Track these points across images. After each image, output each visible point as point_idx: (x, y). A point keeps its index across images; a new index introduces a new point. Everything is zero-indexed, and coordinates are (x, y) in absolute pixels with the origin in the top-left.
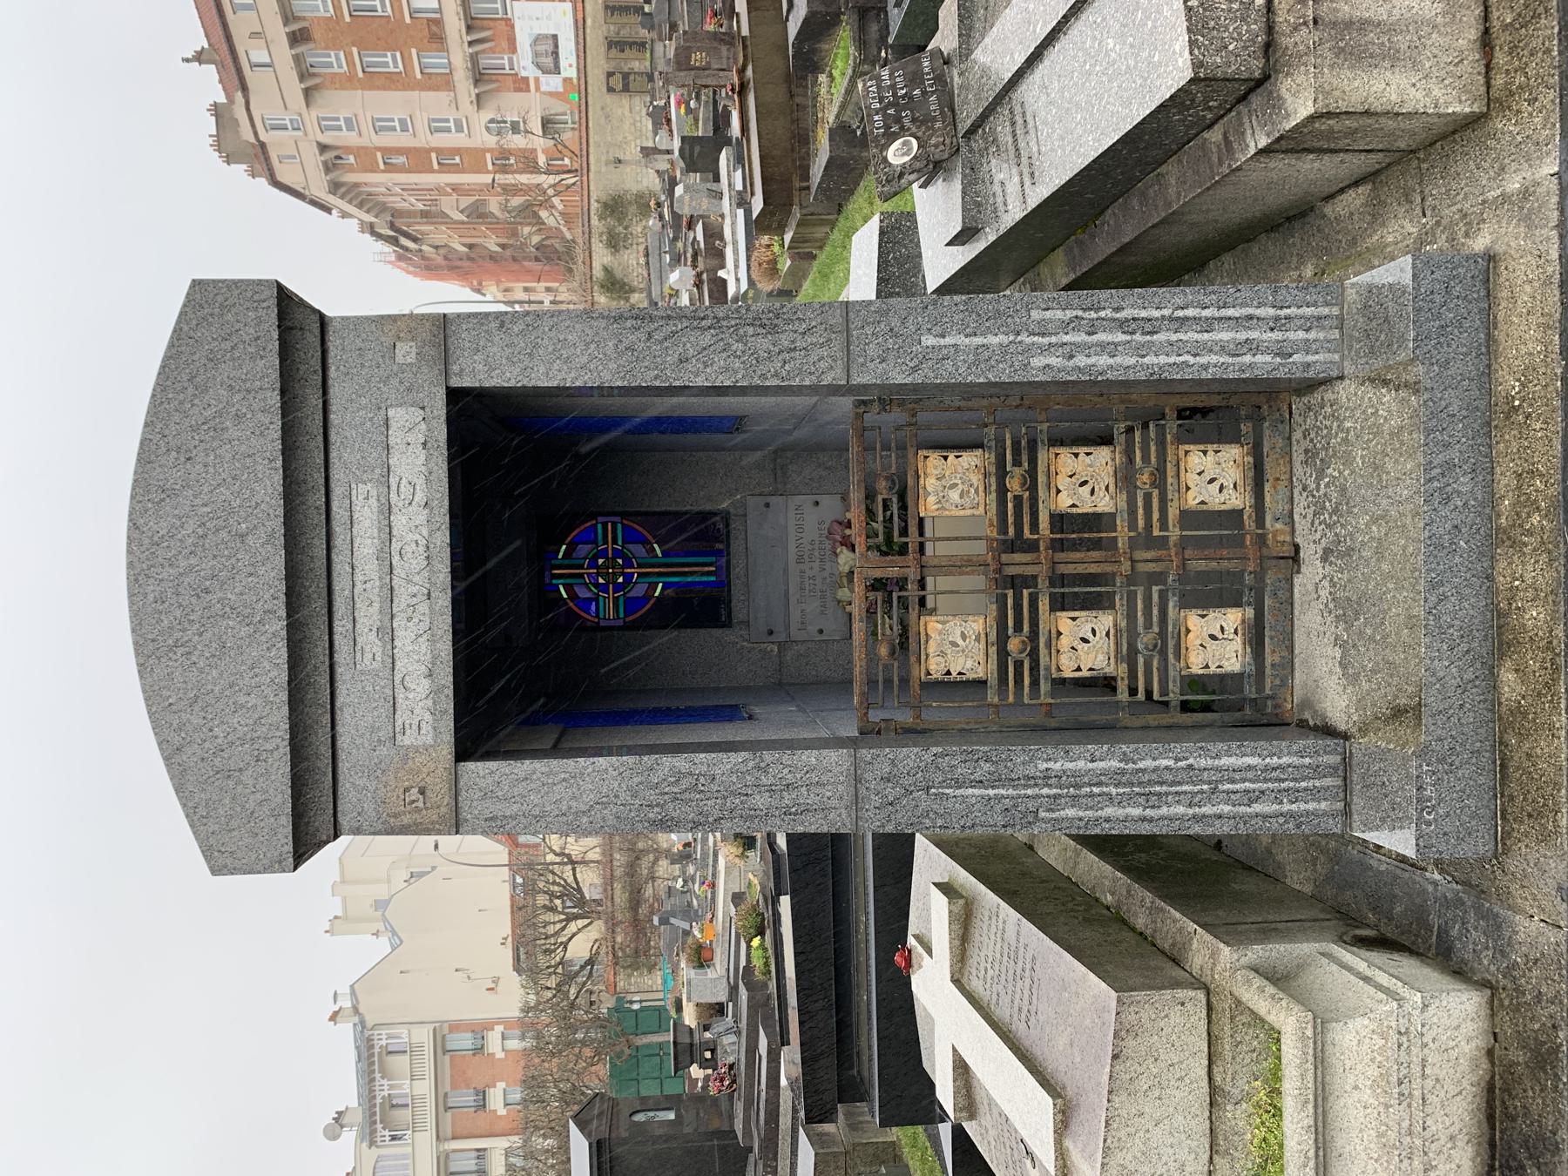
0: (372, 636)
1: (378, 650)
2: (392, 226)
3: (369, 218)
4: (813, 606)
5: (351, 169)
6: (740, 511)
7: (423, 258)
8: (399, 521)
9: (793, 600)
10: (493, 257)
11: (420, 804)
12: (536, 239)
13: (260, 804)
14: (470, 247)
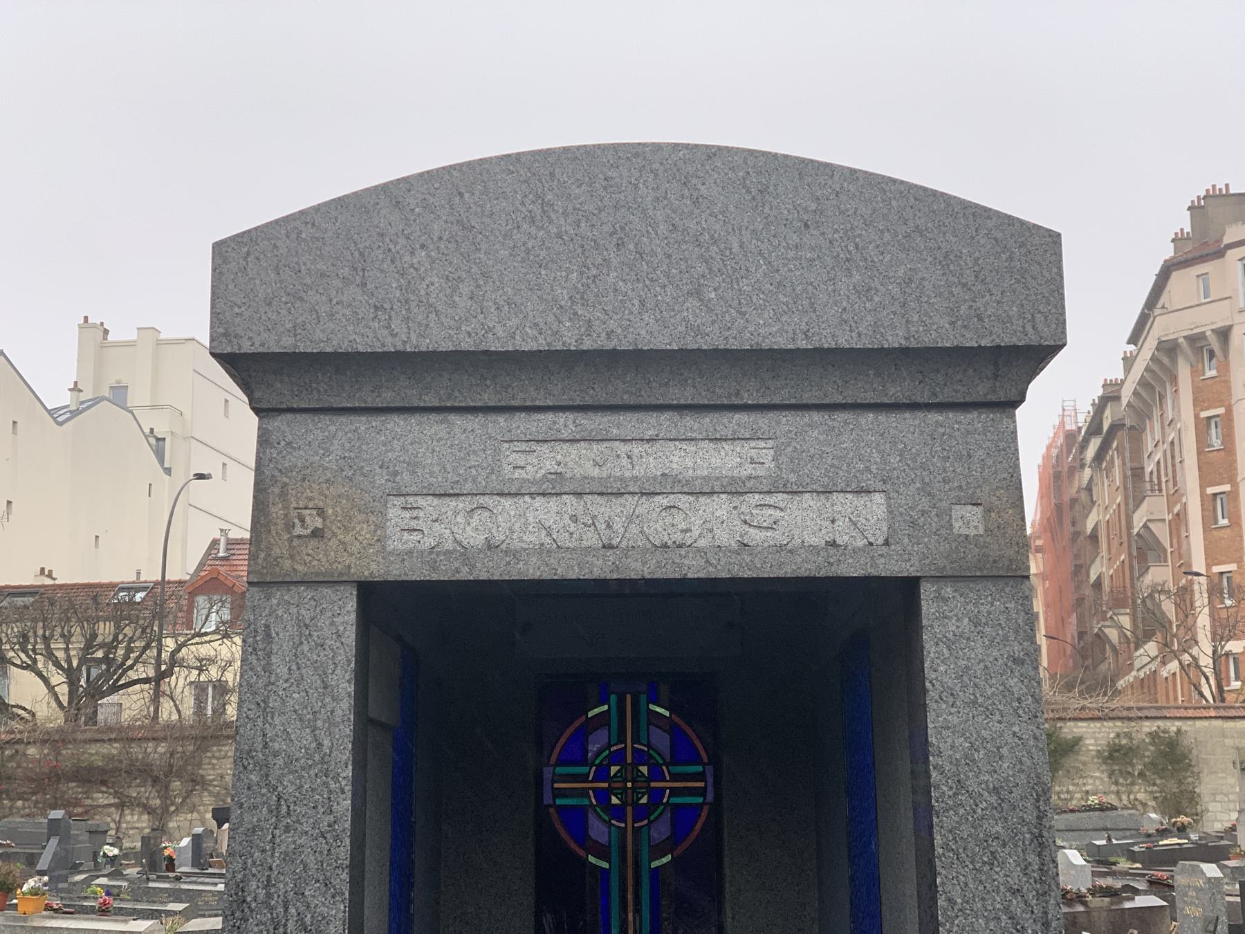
0: (550, 466)
1: (530, 473)
2: (1114, 428)
3: (1126, 394)
5: (1196, 372)
7: (1071, 471)
8: (720, 507)
10: (1080, 570)
11: (298, 530)
12: (1113, 634)
13: (313, 310)
14: (1094, 537)
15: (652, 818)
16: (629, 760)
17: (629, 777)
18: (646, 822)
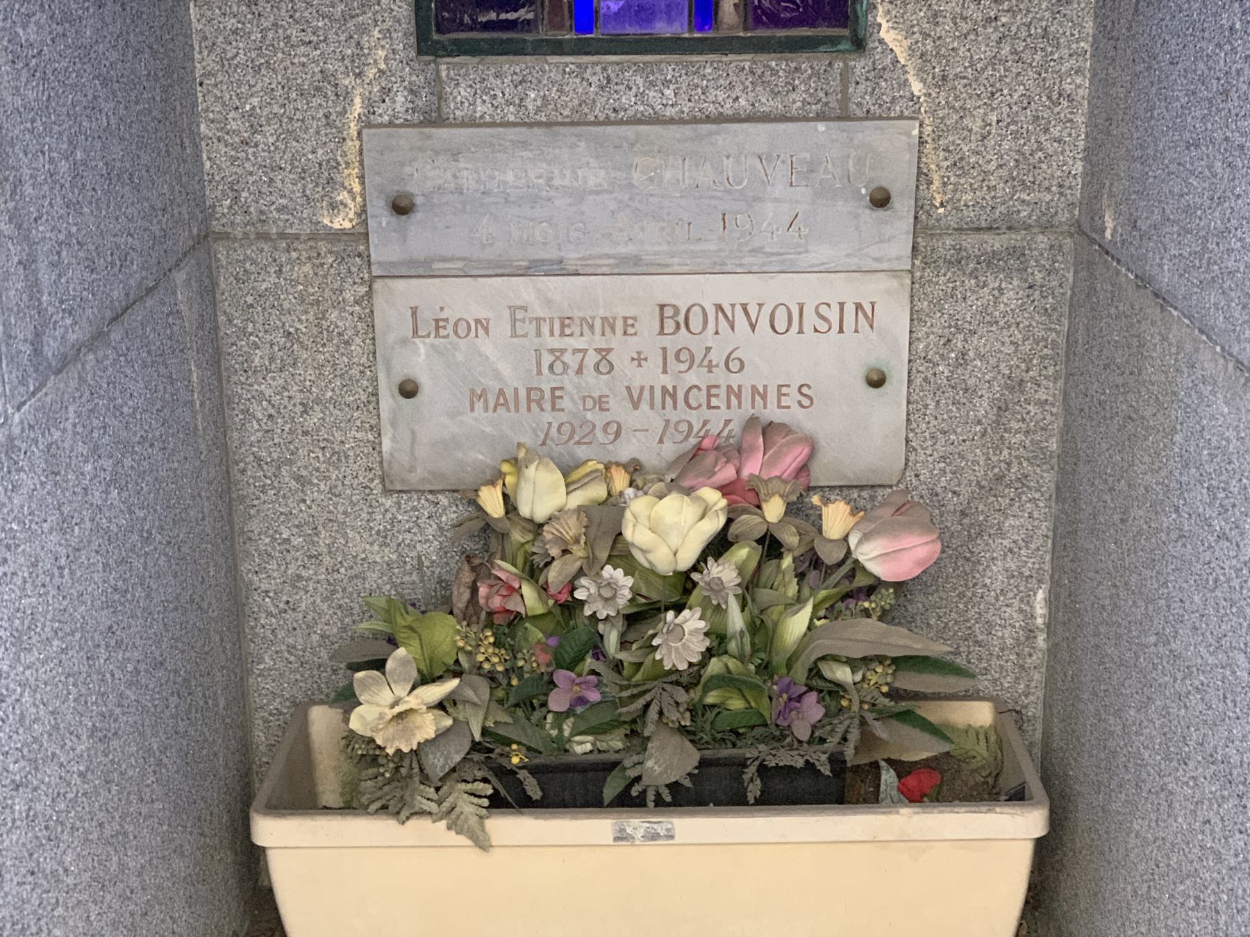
4: (500, 359)
6: (860, 94)
9: (524, 290)
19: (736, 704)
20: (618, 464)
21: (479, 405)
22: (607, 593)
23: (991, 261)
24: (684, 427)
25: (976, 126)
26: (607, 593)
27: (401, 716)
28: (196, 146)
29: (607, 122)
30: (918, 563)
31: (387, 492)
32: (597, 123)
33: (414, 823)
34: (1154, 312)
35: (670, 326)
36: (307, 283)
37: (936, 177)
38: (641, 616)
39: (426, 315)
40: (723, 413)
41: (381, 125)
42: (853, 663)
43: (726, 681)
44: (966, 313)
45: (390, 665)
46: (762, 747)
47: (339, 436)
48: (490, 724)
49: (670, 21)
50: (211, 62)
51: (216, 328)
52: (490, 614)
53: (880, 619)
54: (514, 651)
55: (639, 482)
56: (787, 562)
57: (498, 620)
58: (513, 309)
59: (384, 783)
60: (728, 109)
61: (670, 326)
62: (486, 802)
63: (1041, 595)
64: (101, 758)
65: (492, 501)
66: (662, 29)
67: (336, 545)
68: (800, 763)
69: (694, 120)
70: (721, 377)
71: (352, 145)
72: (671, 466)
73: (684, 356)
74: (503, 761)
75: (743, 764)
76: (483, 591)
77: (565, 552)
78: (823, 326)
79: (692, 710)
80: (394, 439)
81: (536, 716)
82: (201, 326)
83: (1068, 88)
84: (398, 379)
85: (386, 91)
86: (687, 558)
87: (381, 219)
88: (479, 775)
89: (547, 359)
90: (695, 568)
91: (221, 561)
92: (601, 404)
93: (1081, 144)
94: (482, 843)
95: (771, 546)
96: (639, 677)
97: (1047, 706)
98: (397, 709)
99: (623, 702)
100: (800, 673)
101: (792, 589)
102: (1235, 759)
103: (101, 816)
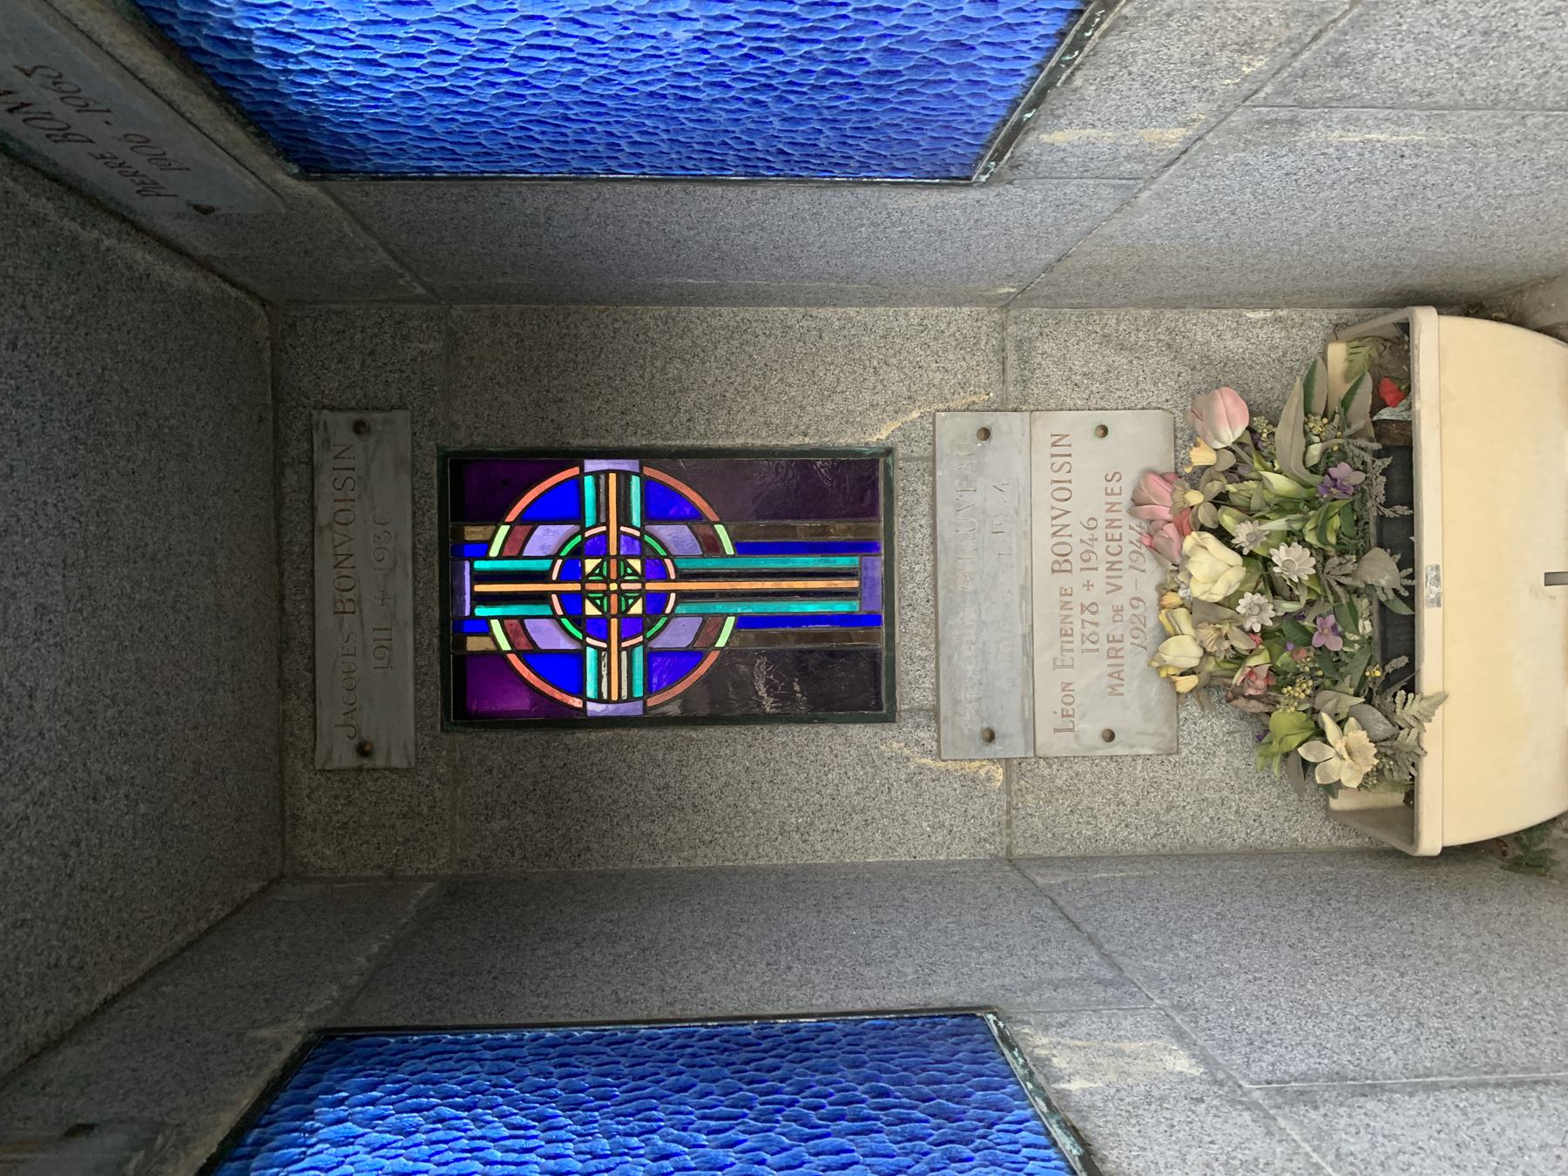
4: (1089, 674)
6: (919, 450)
9: (1042, 660)
15: (662, 553)
16: (576, 587)
17: (602, 587)
18: (668, 562)
19: (1336, 522)
20: (1160, 600)
21: (1120, 690)
22: (1256, 610)
23: (1024, 361)
24: (1134, 556)
25: (939, 376)
26: (1259, 611)
27: (1350, 754)
28: (954, 863)
29: (936, 606)
30: (1236, 402)
31: (1178, 752)
32: (936, 613)
33: (1425, 746)
34: (1069, 262)
35: (1066, 566)
36: (1038, 798)
37: (970, 399)
38: (1273, 587)
39: (1060, 722)
40: (1125, 531)
41: (939, 747)
42: (1309, 443)
43: (1321, 531)
44: (1057, 374)
45: (1310, 759)
46: (1369, 504)
47: (1140, 782)
48: (1352, 691)
49: (874, 568)
50: (902, 850)
51: (1068, 858)
52: (1269, 687)
53: (1275, 426)
54: (1298, 673)
55: (1174, 586)
56: (1231, 488)
57: (1273, 682)
58: (1055, 667)
59: (1398, 767)
60: (927, 531)
61: (1066, 566)
62: (1411, 696)
63: (1250, 315)
64: (1387, 960)
65: (1187, 684)
66: (879, 572)
67: (1216, 784)
68: (1384, 479)
69: (935, 552)
70: (1100, 533)
71: (951, 766)
72: (1161, 564)
73: (1086, 557)
74: (1379, 682)
75: (1382, 518)
76: (1251, 692)
77: (1226, 637)
78: (1067, 467)
79: (1341, 554)
80: (1143, 746)
81: (1344, 658)
82: (1069, 869)
83: (917, 320)
84: (1100, 742)
85: (917, 743)
86: (1235, 558)
87: (997, 749)
88: (1390, 699)
89: (1089, 645)
90: (1239, 551)
91: (1227, 864)
92: (1118, 611)
93: (952, 309)
94: (1442, 698)
95: (1221, 500)
96: (1318, 590)
97: (1330, 306)
98: (1345, 756)
99: (1337, 600)
100: (1315, 479)
101: (1252, 484)
102: (1396, 193)
103: (1430, 963)
